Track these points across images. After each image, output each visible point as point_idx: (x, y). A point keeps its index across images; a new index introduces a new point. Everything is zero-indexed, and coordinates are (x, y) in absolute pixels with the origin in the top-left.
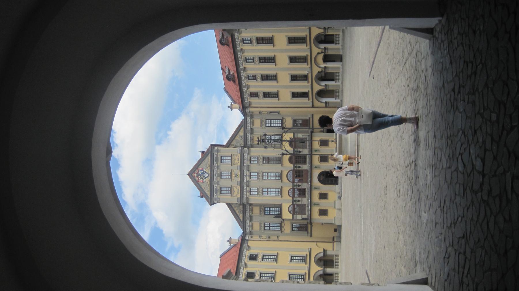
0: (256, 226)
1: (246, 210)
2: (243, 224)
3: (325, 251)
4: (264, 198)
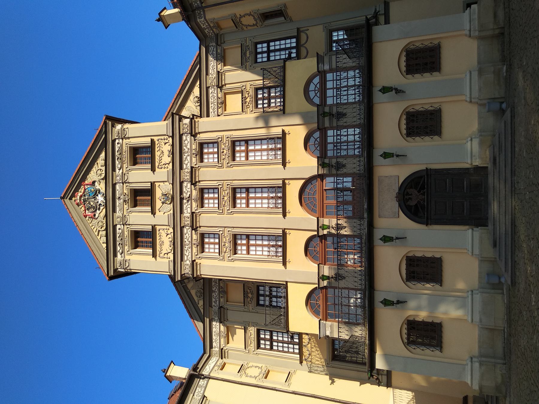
4: (237, 264)
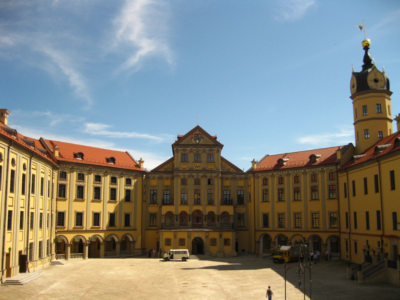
0: (154, 183)
1: (167, 174)
2: (155, 171)
3: (134, 242)
